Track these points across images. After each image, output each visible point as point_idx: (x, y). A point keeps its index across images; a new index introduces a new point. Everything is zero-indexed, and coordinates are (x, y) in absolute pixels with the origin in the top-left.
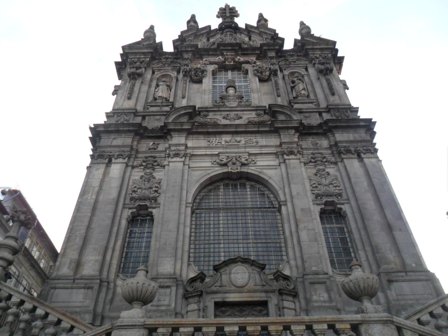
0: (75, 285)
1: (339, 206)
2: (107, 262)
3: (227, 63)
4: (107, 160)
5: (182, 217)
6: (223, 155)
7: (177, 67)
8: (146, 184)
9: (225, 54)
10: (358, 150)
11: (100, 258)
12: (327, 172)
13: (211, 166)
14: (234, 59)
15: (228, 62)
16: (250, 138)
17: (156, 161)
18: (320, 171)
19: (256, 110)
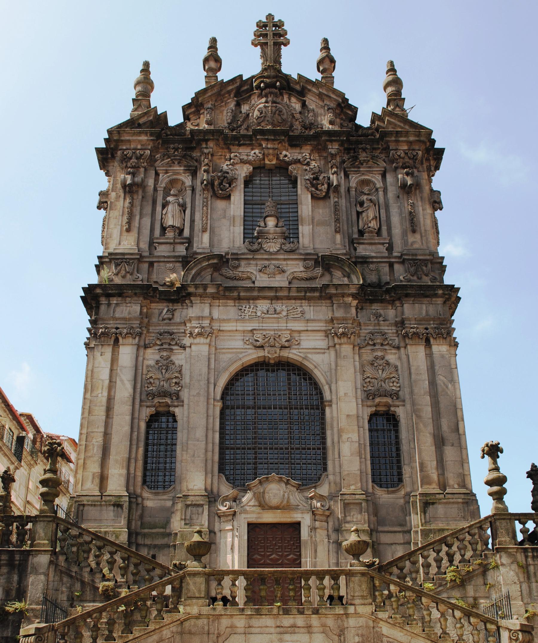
2: (132, 475)
3: (267, 162)
4: (113, 339)
5: (211, 420)
6: (258, 332)
7: (191, 166)
8: (164, 373)
9: (264, 146)
10: (427, 334)
11: (124, 472)
13: (242, 347)
14: (277, 155)
15: (269, 160)
17: (174, 339)
18: (377, 359)
19: (305, 260)
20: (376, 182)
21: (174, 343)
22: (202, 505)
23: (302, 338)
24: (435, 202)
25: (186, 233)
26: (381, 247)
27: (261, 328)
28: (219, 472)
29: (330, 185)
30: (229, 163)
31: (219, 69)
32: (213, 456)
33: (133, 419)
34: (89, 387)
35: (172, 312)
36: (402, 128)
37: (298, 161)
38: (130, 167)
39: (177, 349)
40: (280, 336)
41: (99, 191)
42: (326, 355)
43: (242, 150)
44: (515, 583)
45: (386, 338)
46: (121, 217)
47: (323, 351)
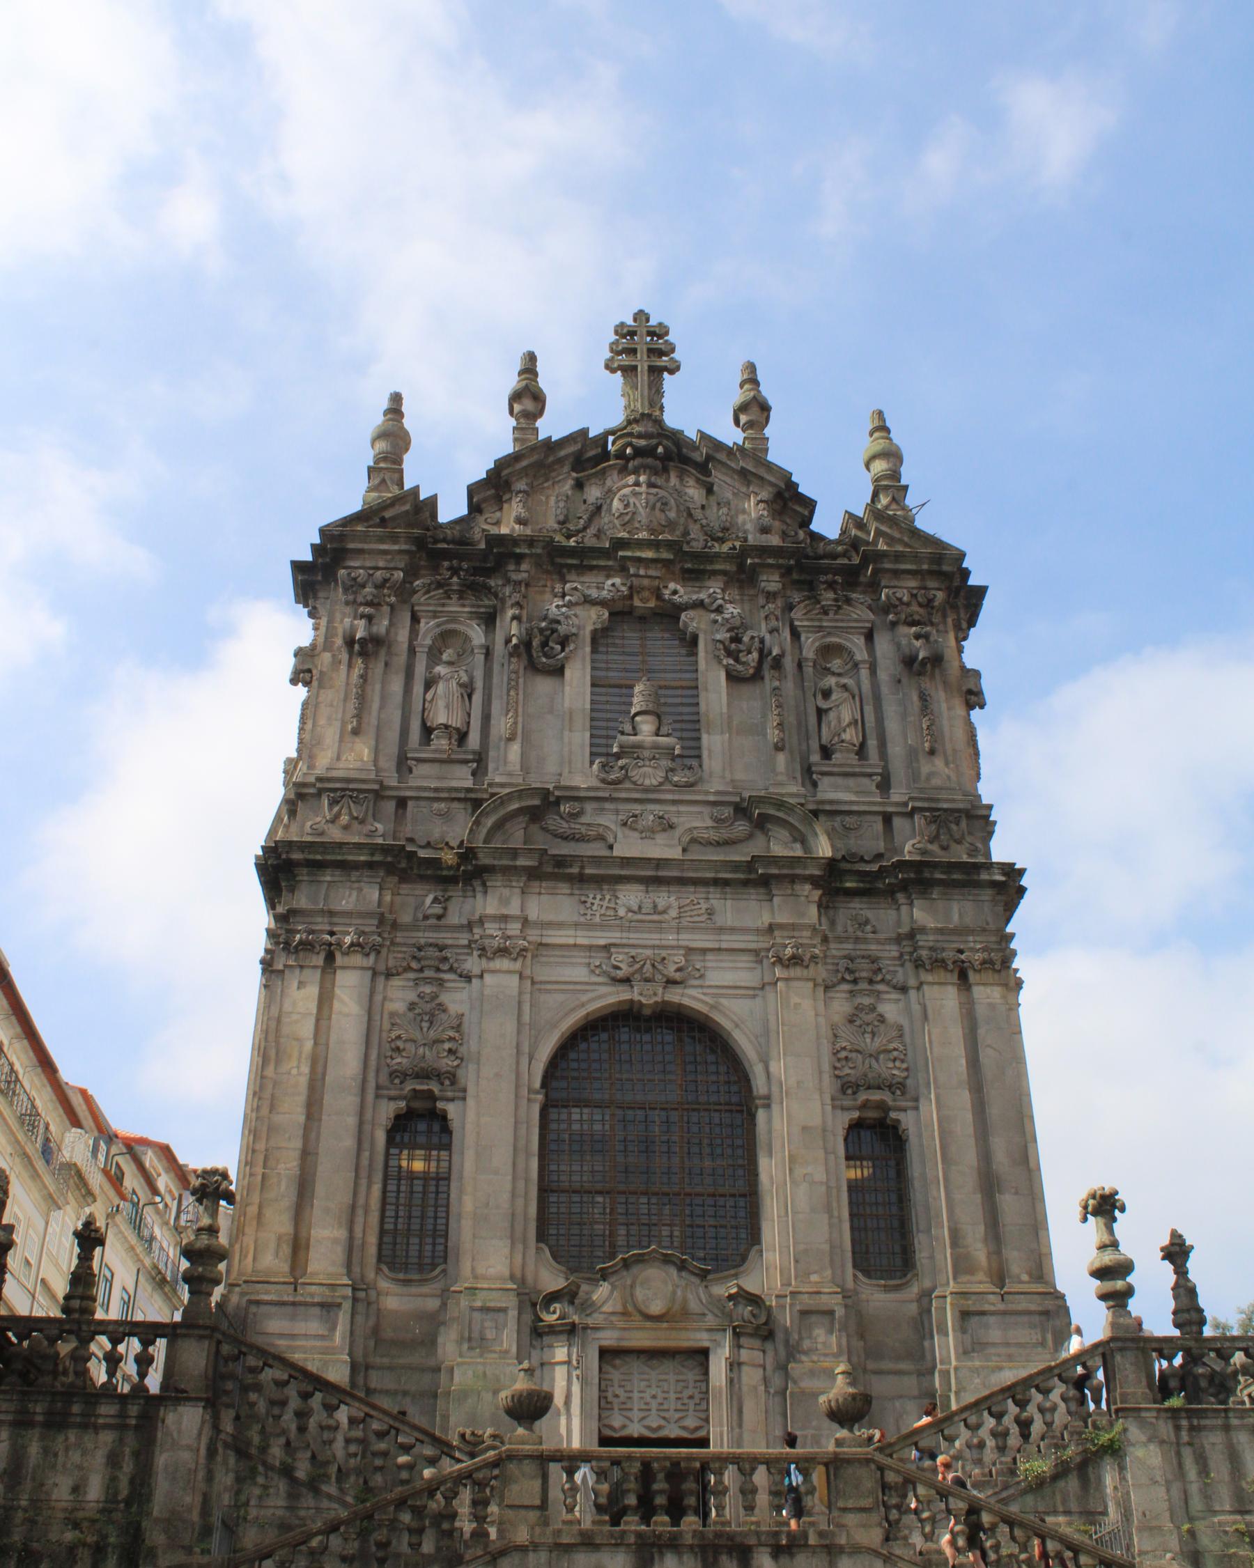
0: (299, 1298)
1: (893, 1115)
2: (358, 1242)
3: (637, 603)
4: (322, 956)
5: (523, 1131)
9: (632, 571)
10: (963, 962)
11: (342, 1234)
12: (881, 1016)
13: (586, 980)
14: (659, 589)
16: (692, 897)
18: (862, 1010)
20: (854, 650)
21: (446, 967)
22: (503, 1310)
23: (709, 964)
24: (970, 692)
25: (474, 740)
26: (865, 781)
27: (624, 941)
28: (538, 1241)
29: (763, 654)
30: (561, 603)
31: (541, 412)
32: (526, 1206)
33: (361, 1123)
34: (272, 1053)
35: (443, 901)
36: (906, 545)
37: (700, 605)
38: (361, 604)
39: (454, 981)
40: (664, 959)
41: (295, 647)
42: (758, 1001)
43: (590, 578)
45: (880, 969)
46: (341, 704)
47: (751, 992)
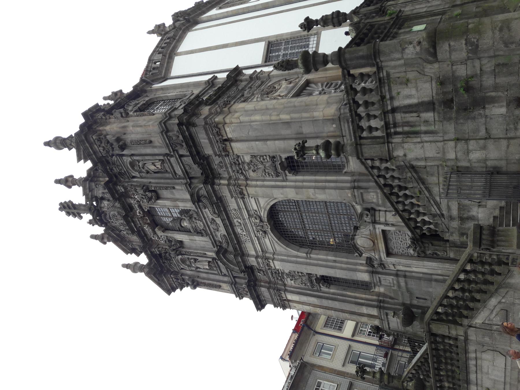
3: (149, 221)
23: (252, 209)
25: (210, 260)
44: (423, 146)
